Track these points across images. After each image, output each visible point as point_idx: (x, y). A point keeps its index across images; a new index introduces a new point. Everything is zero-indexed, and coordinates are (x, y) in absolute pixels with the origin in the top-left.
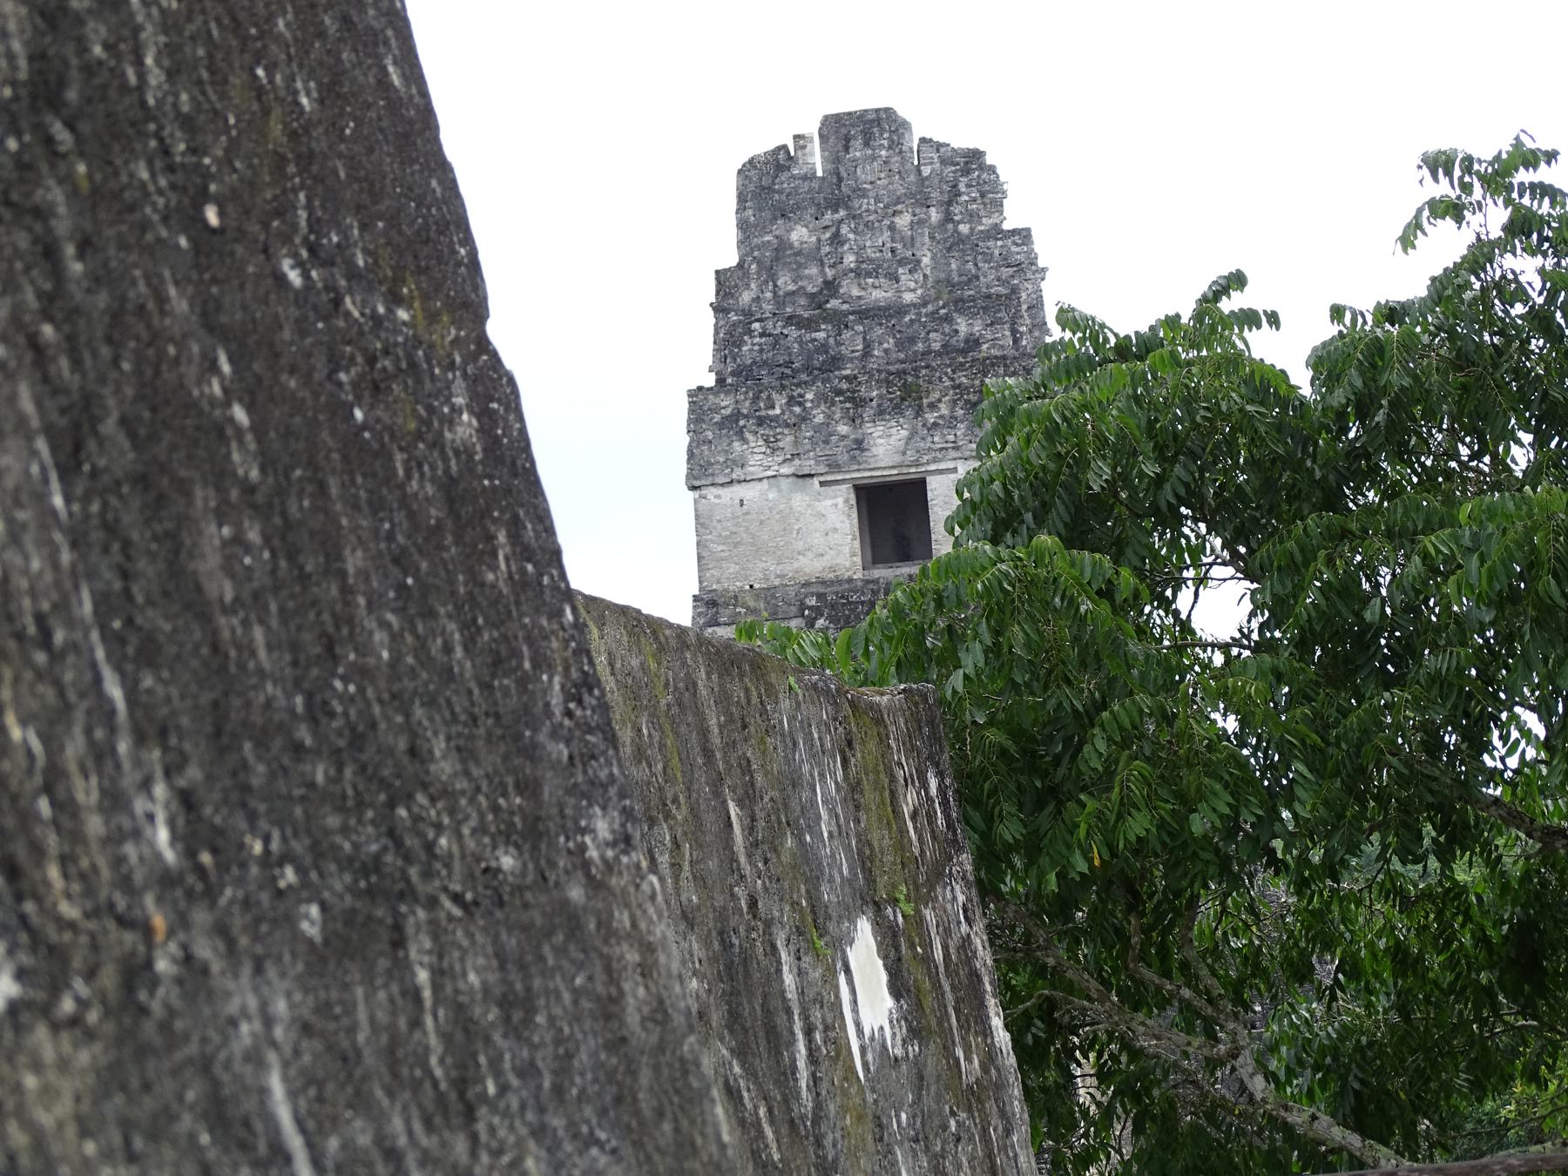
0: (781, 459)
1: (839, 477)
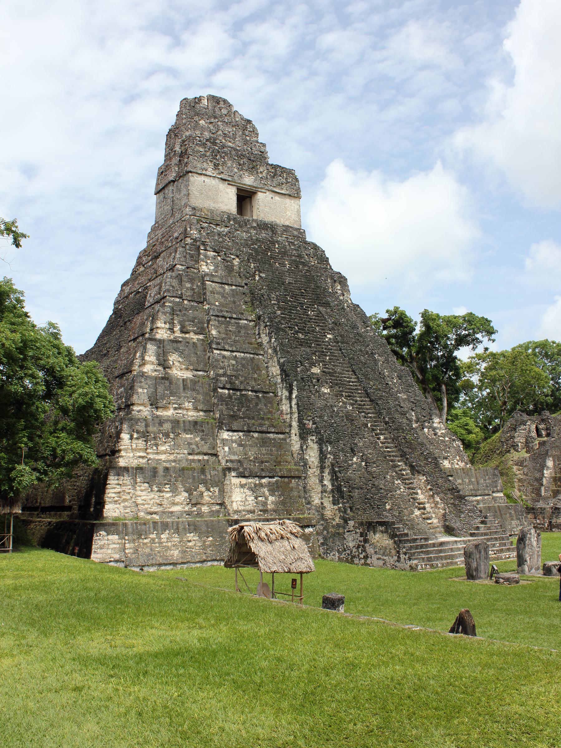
0: (217, 172)
1: (234, 184)
